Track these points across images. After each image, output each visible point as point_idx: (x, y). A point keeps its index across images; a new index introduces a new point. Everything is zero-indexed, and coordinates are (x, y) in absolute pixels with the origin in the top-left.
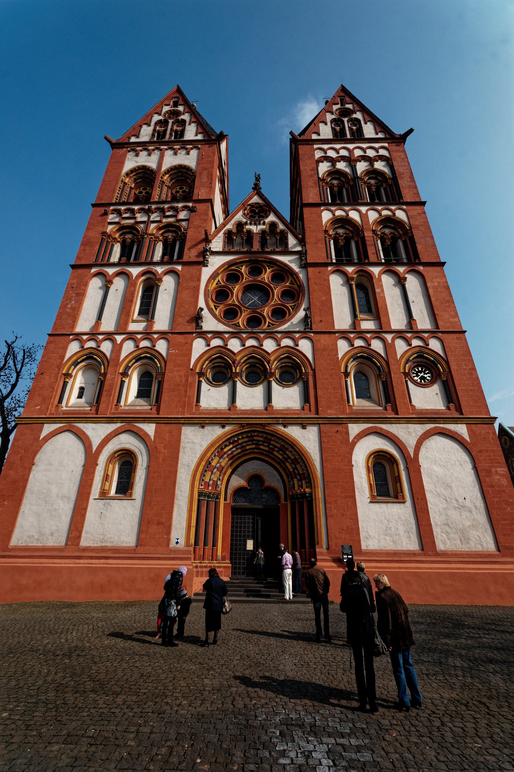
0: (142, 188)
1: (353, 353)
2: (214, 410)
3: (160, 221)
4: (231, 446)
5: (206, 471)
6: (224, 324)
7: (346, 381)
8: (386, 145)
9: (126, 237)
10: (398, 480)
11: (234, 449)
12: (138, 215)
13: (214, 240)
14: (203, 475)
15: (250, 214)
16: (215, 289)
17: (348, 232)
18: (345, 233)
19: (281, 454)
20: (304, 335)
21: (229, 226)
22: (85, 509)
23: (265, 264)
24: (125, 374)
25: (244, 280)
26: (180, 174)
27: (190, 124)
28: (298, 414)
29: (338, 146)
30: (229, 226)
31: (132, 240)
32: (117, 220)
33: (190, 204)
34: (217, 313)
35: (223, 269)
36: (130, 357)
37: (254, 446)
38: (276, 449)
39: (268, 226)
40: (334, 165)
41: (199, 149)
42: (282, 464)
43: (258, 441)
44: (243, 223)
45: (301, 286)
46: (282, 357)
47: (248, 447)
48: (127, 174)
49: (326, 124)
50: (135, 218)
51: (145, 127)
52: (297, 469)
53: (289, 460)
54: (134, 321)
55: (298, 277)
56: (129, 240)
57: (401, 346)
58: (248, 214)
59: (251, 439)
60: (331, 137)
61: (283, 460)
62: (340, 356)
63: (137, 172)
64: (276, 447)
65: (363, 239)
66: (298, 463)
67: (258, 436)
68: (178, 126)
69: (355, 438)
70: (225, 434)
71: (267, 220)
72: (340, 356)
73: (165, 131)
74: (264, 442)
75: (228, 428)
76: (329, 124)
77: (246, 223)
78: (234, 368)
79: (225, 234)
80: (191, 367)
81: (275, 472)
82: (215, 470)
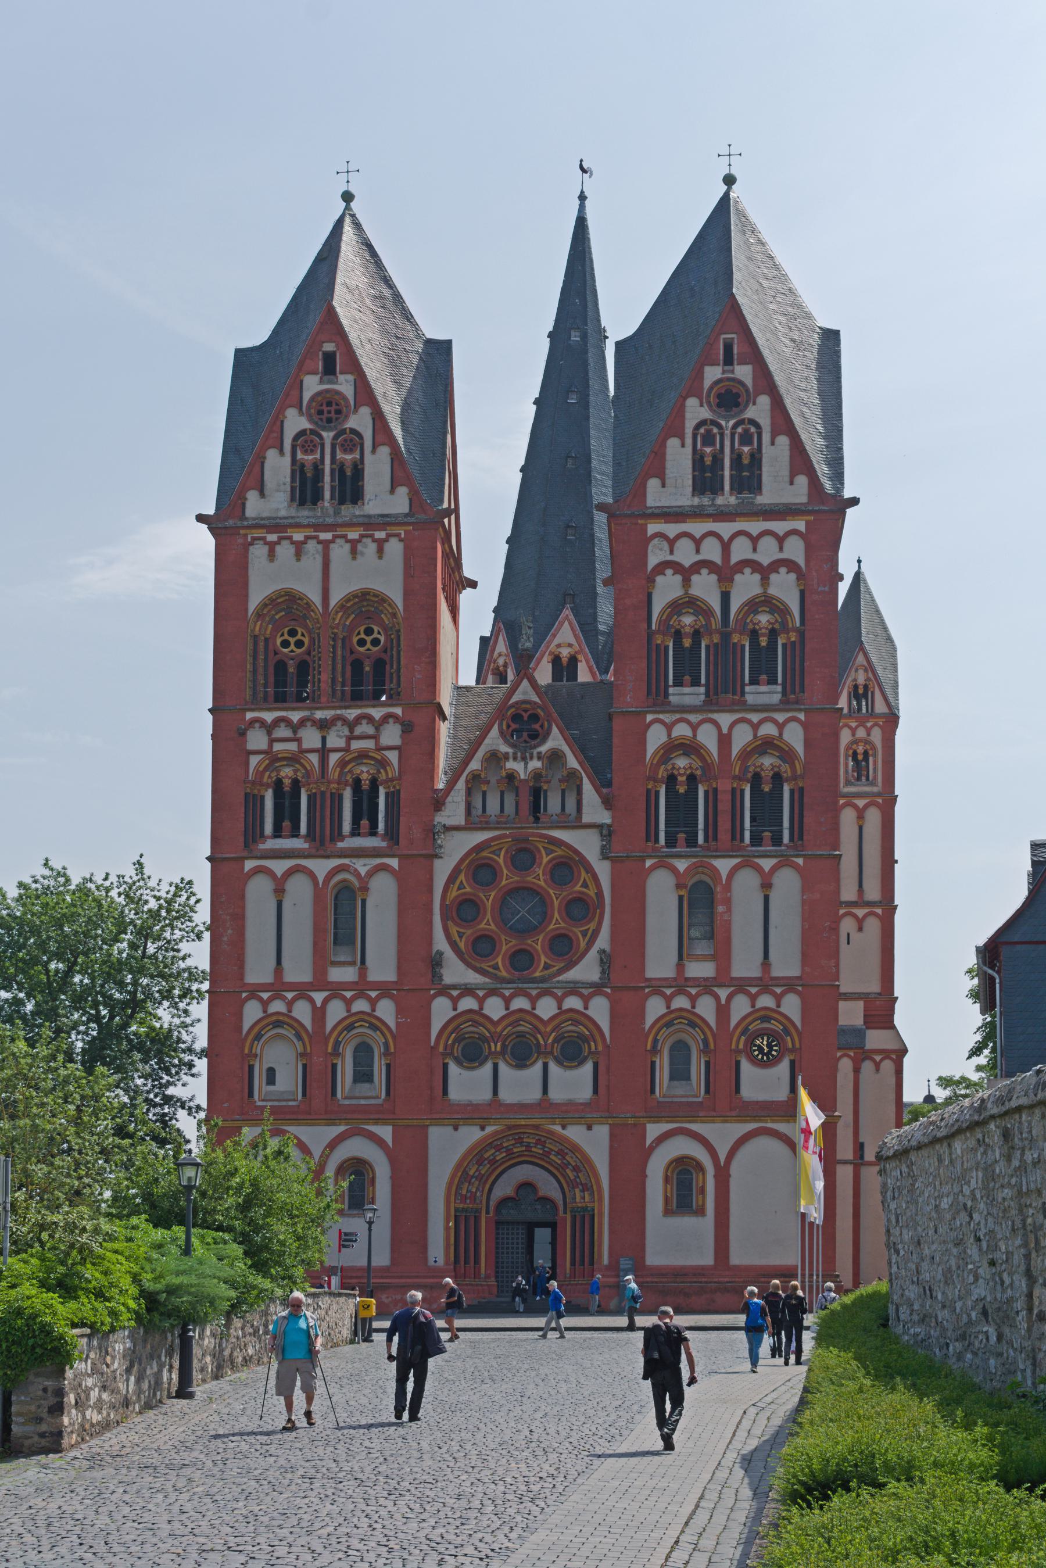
1: (667, 1018)
2: (468, 1105)
3: (347, 749)
7: (653, 1063)
8: (800, 525)
10: (702, 1191)
13: (449, 799)
14: (459, 1188)
15: (514, 726)
18: (690, 767)
20: (597, 989)
21: (475, 765)
24: (336, 1053)
25: (504, 882)
26: (365, 603)
27: (374, 450)
29: (697, 528)
32: (264, 746)
33: (398, 711)
34: (462, 945)
36: (340, 1028)
40: (686, 582)
41: (401, 540)
44: (499, 755)
45: (600, 894)
48: (259, 615)
49: (683, 446)
50: (299, 740)
51: (272, 454)
54: (334, 964)
58: (509, 726)
62: (649, 1021)
65: (715, 790)
68: (345, 451)
71: (543, 749)
75: (489, 1129)
76: (689, 441)
78: (492, 1045)
79: (467, 782)
80: (432, 1044)
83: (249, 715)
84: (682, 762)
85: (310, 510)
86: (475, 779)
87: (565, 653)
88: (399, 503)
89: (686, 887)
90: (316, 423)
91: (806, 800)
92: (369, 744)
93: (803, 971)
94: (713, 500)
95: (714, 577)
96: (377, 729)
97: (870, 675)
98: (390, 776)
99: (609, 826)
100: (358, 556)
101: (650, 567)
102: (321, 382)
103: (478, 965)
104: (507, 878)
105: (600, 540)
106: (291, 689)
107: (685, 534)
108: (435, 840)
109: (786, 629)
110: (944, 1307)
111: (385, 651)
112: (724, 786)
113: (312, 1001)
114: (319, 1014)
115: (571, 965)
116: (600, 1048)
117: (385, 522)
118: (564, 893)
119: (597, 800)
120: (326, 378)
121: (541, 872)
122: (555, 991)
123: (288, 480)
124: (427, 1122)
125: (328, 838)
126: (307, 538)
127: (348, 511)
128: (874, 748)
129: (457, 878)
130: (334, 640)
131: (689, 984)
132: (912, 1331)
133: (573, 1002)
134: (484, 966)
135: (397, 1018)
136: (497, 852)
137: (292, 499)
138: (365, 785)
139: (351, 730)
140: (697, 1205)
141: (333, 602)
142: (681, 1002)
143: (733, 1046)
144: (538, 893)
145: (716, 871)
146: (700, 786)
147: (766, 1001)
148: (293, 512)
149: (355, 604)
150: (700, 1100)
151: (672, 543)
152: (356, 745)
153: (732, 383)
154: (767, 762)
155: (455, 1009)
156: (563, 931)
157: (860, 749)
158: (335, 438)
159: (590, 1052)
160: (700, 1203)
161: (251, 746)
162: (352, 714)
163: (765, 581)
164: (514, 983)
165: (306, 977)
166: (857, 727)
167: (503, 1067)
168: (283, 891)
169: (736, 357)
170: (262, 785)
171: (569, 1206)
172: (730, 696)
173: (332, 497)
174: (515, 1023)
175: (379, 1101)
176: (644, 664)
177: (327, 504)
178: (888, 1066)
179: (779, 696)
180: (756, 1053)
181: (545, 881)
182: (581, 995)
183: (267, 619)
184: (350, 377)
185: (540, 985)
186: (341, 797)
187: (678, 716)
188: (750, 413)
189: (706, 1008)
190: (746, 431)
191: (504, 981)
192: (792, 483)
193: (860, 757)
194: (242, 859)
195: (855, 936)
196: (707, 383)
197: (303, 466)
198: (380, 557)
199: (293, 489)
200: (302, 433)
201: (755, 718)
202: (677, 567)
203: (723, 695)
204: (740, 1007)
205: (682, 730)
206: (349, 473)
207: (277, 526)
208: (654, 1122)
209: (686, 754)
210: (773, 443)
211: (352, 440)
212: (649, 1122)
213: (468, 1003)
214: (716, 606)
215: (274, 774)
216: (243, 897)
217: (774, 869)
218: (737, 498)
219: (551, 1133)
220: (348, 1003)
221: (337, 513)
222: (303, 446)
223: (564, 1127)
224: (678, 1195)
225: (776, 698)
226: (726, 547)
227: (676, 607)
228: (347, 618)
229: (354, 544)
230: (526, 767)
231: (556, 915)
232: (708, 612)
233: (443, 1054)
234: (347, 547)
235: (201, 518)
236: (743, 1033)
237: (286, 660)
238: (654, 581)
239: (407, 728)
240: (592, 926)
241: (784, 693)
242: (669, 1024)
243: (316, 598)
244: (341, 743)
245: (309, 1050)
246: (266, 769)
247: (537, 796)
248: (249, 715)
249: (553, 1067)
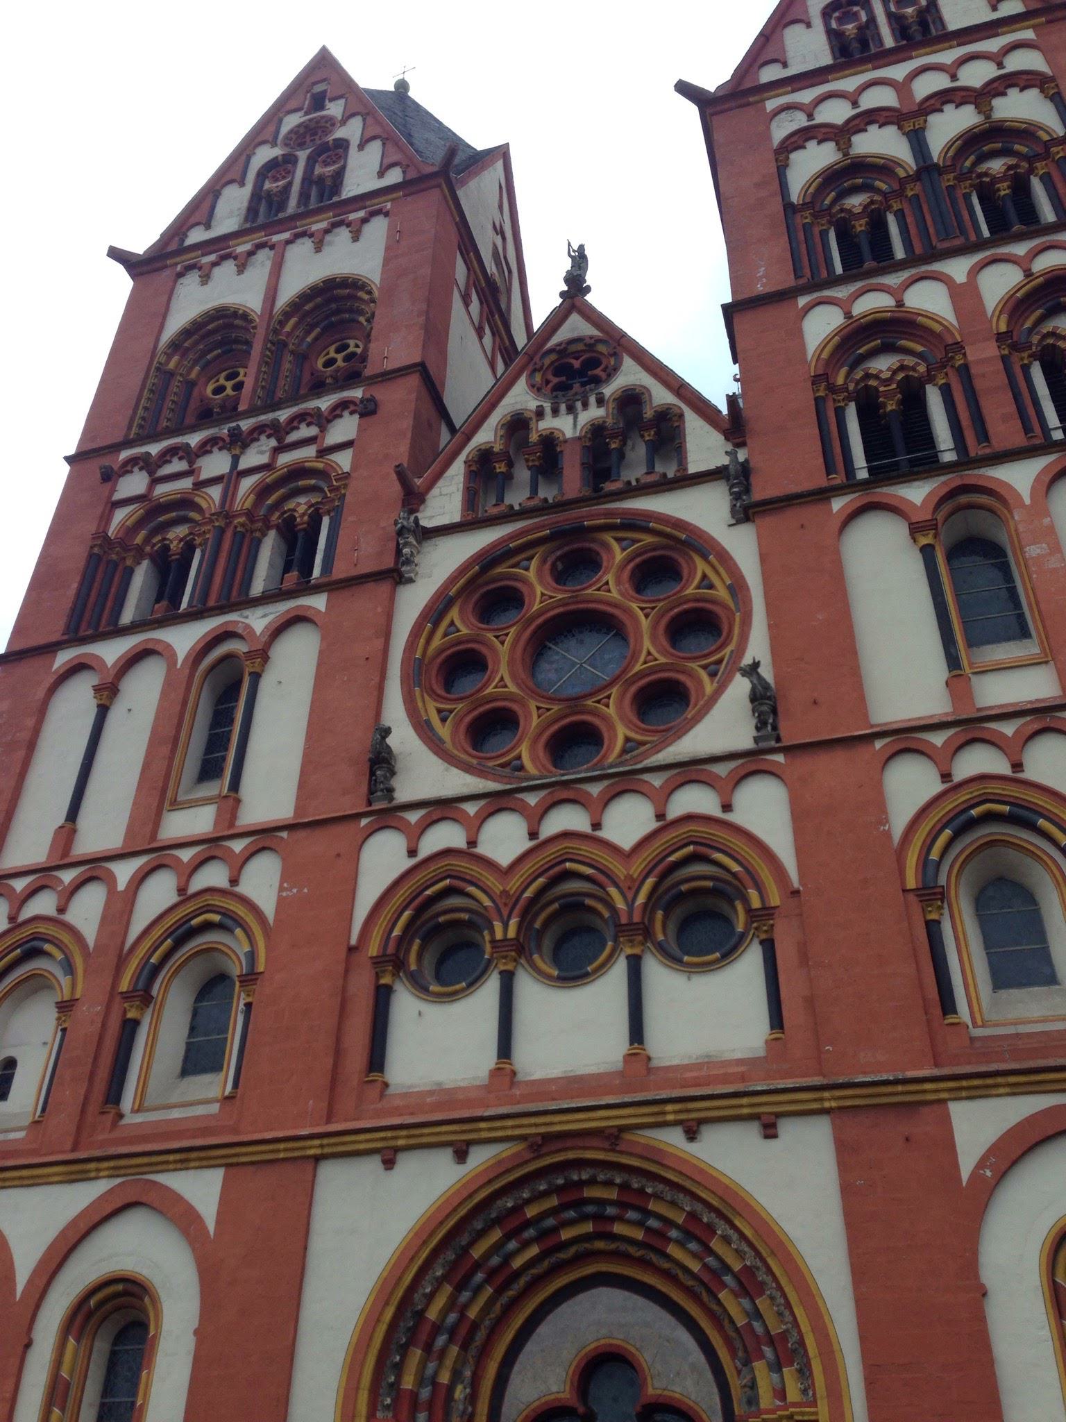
0: (224, 374)
1: (948, 805)
2: (431, 1093)
4: (496, 1235)
5: (404, 1350)
6: (467, 768)
7: (933, 930)
11: (512, 1245)
13: (435, 491)
15: (555, 380)
16: (441, 651)
17: (910, 361)
19: (695, 1255)
21: (486, 436)
23: (608, 538)
24: (143, 995)
26: (334, 306)
27: (361, 147)
28: (743, 1078)
29: (849, 84)
30: (486, 436)
31: (186, 543)
33: (357, 393)
34: (444, 731)
35: (462, 581)
37: (588, 1227)
38: (674, 1234)
39: (611, 405)
41: (387, 214)
42: (705, 1297)
43: (601, 1202)
44: (527, 414)
45: (738, 587)
46: (672, 858)
47: (566, 1235)
49: (809, 25)
52: (758, 1315)
53: (728, 1279)
54: (176, 805)
55: (725, 558)
58: (548, 382)
60: (826, 59)
61: (706, 1278)
65: (965, 372)
66: (761, 1287)
67: (592, 1182)
69: (981, 1164)
71: (610, 390)
73: (287, 188)
75: (480, 1157)
77: (540, 413)
78: (498, 926)
80: (353, 941)
81: (684, 1336)
82: (441, 1340)
84: (883, 364)
92: (309, 452)
113: (110, 880)
116: (775, 899)
122: (646, 777)
135: (281, 889)
136: (525, 563)
138: (302, 520)
152: (285, 459)
155: (412, 853)
161: (117, 496)
175: (215, 1108)
182: (709, 782)
186: (256, 545)
194: (51, 648)
209: (888, 348)
213: (445, 836)
219: (655, 1154)
223: (692, 1135)
228: (308, 333)
231: (647, 644)
233: (378, 962)
246: (139, 524)
248: (124, 455)
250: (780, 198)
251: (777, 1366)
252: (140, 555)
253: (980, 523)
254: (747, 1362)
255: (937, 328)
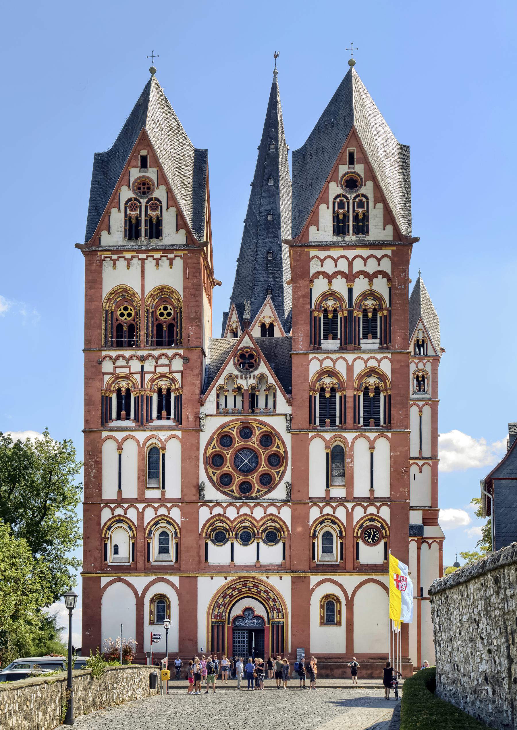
0: (123, 307)
2: (218, 566)
3: (154, 373)
6: (222, 492)
7: (314, 544)
8: (388, 252)
9: (121, 386)
10: (339, 613)
12: (131, 363)
15: (241, 361)
18: (332, 383)
20: (285, 502)
21: (221, 381)
22: (143, 632)
24: (150, 537)
25: (236, 445)
26: (163, 293)
29: (335, 253)
33: (181, 351)
34: (215, 479)
37: (247, 589)
44: (234, 376)
45: (286, 452)
47: (243, 590)
48: (109, 300)
49: (328, 208)
50: (129, 367)
52: (275, 605)
54: (148, 488)
55: (283, 443)
56: (123, 390)
57: (359, 513)
58: (238, 361)
59: (245, 585)
63: (116, 293)
64: (262, 590)
65: (345, 396)
66: (277, 602)
68: (152, 210)
70: (227, 584)
71: (256, 373)
72: (311, 523)
74: (254, 587)
77: (237, 377)
78: (231, 533)
79: (217, 390)
82: (221, 606)
83: (104, 353)
84: (328, 381)
85: (134, 242)
86: (221, 388)
87: (267, 321)
88: (180, 239)
89: (330, 448)
90: (137, 195)
91: (392, 402)
92: (166, 370)
93: (391, 494)
94: (344, 238)
95: (344, 280)
96: (170, 361)
97: (425, 334)
98: (177, 387)
99: (290, 415)
100: (159, 267)
101: (311, 275)
102: (140, 172)
103: (223, 490)
104: (238, 443)
105: (285, 260)
106: (125, 340)
107: (329, 257)
108: (200, 422)
109: (381, 308)
110: (464, 675)
111: (174, 319)
112: (350, 393)
113: (137, 509)
114: (141, 516)
115: (270, 490)
116: (286, 535)
117: (172, 249)
118: (267, 451)
119: (284, 401)
120: (142, 170)
121: (255, 440)
122: (263, 504)
123: (123, 225)
124: (197, 575)
125: (145, 420)
126: (133, 257)
127: (154, 242)
128: (427, 374)
129: (211, 443)
130: (147, 313)
131: (332, 500)
132: (448, 689)
133: (272, 510)
134: (226, 490)
135: (181, 518)
136: (233, 429)
137: (125, 236)
138: (164, 392)
139: (157, 362)
140: (337, 621)
141: (146, 293)
142: (328, 510)
143: (355, 535)
144: (254, 451)
145: (345, 439)
146: (337, 393)
147: (372, 510)
148: (125, 243)
149: (158, 293)
150: (338, 563)
151: (322, 261)
152: (159, 370)
153: (353, 175)
154: (372, 380)
155: (211, 514)
156: (267, 472)
157: (420, 375)
158: (147, 202)
159: (281, 537)
160: (338, 619)
161: (104, 370)
162: (157, 353)
163: (371, 282)
164: (242, 499)
165: (135, 496)
166: (418, 362)
167: (236, 545)
168: (122, 449)
169: (355, 160)
170: (110, 391)
171: (271, 620)
172: (352, 345)
173: (146, 235)
174: (241, 522)
175: (172, 563)
176: (308, 328)
177: (143, 239)
178: (435, 546)
179: (378, 345)
180: (367, 538)
181: (257, 445)
183: (113, 301)
184: (155, 170)
185: (255, 501)
187: (326, 355)
188: (363, 191)
189: (341, 514)
190: (361, 201)
191: (236, 498)
192: (384, 229)
193: (420, 379)
195: (418, 475)
196: (340, 175)
197: (130, 218)
198: (171, 268)
199: (125, 230)
200: (130, 200)
201: (366, 356)
202: (325, 275)
203: (349, 345)
204: (359, 513)
205: (328, 364)
206: (154, 221)
207: (117, 250)
208: (314, 575)
210: (375, 208)
211: (156, 204)
212: (312, 575)
214: (345, 295)
215: (117, 385)
216: (101, 452)
217: (376, 439)
218: (356, 237)
220: (156, 510)
221: (148, 243)
222: (131, 207)
223: (268, 578)
224: (327, 615)
225: (376, 346)
226: (350, 264)
227: (325, 296)
228: (154, 301)
229: (157, 260)
230: (247, 383)
231: (263, 463)
232: (340, 299)
233: (205, 538)
234: (155, 261)
235: (77, 246)
236: (360, 528)
237: (122, 323)
238: (313, 282)
239: (186, 361)
240: (282, 469)
241: (381, 343)
242: (322, 523)
243: (138, 291)
244: (152, 369)
245: (135, 536)
246: (113, 383)
247: (253, 398)
249: (262, 545)
250: (309, 306)
251: (278, 612)
252: (113, 392)
253: (340, 444)
254: (273, 611)
255: (342, 380)
